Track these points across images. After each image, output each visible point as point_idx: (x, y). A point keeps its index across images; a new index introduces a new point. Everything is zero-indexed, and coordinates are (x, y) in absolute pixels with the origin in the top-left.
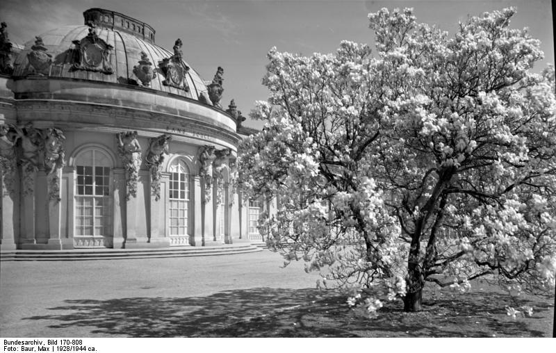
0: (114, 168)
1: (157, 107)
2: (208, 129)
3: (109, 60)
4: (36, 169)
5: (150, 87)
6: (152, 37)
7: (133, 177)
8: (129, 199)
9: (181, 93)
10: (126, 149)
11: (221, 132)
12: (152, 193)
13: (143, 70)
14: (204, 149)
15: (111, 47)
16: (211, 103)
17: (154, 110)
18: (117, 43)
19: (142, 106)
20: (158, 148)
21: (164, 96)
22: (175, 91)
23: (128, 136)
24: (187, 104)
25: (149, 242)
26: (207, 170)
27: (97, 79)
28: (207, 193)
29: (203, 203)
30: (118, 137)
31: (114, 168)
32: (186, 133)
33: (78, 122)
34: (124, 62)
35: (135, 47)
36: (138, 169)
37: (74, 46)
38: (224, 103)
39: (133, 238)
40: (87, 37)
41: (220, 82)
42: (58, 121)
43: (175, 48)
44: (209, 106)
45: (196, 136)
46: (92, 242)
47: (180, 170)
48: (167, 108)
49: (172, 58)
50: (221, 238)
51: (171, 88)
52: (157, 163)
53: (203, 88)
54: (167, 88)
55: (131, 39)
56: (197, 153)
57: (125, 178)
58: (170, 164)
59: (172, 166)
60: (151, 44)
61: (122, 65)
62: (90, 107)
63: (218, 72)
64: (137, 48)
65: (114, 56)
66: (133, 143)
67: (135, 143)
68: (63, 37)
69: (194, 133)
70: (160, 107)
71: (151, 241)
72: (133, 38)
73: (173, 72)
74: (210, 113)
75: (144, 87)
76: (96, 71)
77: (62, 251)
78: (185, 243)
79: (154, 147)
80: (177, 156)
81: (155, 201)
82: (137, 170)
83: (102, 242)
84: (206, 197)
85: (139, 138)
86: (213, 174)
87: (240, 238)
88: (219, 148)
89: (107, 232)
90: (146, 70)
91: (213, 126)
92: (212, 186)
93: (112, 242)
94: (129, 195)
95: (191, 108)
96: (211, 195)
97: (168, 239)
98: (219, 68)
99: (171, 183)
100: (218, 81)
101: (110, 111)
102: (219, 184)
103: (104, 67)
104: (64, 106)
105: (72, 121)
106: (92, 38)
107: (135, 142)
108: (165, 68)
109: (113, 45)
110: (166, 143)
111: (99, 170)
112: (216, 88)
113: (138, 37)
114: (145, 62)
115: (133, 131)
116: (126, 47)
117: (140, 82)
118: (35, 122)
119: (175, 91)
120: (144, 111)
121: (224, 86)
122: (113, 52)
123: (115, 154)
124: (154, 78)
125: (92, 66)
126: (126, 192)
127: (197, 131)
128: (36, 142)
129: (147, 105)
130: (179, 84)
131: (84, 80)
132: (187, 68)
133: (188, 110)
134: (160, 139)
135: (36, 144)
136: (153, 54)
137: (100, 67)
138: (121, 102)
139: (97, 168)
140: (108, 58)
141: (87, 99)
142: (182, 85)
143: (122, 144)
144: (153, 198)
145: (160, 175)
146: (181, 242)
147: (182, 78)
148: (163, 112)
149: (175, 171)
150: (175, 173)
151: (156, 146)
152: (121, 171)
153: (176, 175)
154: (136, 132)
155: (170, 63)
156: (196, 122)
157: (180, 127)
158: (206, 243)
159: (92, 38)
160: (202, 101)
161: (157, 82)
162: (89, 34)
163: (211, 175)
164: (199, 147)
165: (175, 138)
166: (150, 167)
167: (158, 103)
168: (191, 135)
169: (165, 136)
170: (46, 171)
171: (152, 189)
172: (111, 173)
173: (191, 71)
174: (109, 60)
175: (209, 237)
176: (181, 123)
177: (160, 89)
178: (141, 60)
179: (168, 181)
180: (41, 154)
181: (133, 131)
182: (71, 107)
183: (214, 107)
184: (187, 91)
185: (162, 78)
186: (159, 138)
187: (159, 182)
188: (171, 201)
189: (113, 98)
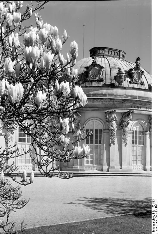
0: (104, 130)
1: (126, 96)
3: (102, 74)
6: (124, 56)
7: (113, 134)
9: (140, 86)
10: (110, 120)
12: (123, 142)
13: (118, 78)
15: (103, 67)
17: (124, 97)
18: (106, 64)
19: (118, 96)
20: (127, 118)
22: (136, 86)
23: (111, 113)
27: (96, 85)
30: (106, 114)
31: (104, 130)
32: (141, 109)
33: (87, 108)
34: (110, 74)
35: (115, 65)
36: (116, 129)
37: (86, 69)
39: (113, 166)
40: (92, 64)
43: (136, 62)
46: (93, 168)
47: (137, 129)
48: (131, 96)
49: (134, 68)
51: (134, 84)
52: (126, 126)
54: (132, 84)
57: (109, 135)
59: (134, 127)
61: (107, 75)
62: (92, 100)
64: (116, 65)
65: (104, 72)
66: (113, 116)
67: (115, 116)
68: (81, 65)
70: (127, 96)
71: (122, 168)
73: (135, 76)
75: (119, 86)
76: (95, 81)
77: (79, 172)
78: (140, 169)
80: (136, 122)
81: (124, 147)
82: (115, 130)
83: (95, 168)
85: (117, 113)
89: (100, 163)
90: (120, 77)
93: (103, 168)
94: (111, 144)
97: (131, 167)
99: (133, 136)
101: (102, 101)
103: (100, 78)
106: (94, 64)
107: (114, 115)
109: (104, 66)
110: (130, 115)
114: (120, 72)
115: (113, 110)
116: (111, 66)
117: (117, 84)
119: (136, 86)
120: (119, 99)
122: (104, 69)
123: (104, 123)
124: (125, 80)
125: (94, 78)
126: (110, 141)
130: (138, 82)
131: (90, 87)
132: (143, 72)
133: (143, 96)
134: (127, 113)
137: (97, 78)
138: (107, 95)
139: (95, 130)
141: (91, 96)
142: (140, 82)
143: (108, 117)
144: (123, 145)
145: (127, 132)
147: (140, 78)
148: (129, 98)
149: (135, 130)
150: (135, 131)
151: (125, 117)
152: (107, 131)
153: (136, 132)
154: (115, 111)
155: (133, 71)
157: (139, 105)
159: (94, 64)
162: (93, 63)
165: (135, 112)
166: (122, 128)
167: (127, 94)
169: (130, 111)
171: (123, 140)
172: (103, 132)
174: (102, 74)
176: (139, 104)
178: (118, 72)
179: (131, 135)
181: (113, 110)
184: (142, 85)
185: (129, 80)
186: (127, 112)
187: (126, 136)
188: (133, 146)
189: (104, 94)
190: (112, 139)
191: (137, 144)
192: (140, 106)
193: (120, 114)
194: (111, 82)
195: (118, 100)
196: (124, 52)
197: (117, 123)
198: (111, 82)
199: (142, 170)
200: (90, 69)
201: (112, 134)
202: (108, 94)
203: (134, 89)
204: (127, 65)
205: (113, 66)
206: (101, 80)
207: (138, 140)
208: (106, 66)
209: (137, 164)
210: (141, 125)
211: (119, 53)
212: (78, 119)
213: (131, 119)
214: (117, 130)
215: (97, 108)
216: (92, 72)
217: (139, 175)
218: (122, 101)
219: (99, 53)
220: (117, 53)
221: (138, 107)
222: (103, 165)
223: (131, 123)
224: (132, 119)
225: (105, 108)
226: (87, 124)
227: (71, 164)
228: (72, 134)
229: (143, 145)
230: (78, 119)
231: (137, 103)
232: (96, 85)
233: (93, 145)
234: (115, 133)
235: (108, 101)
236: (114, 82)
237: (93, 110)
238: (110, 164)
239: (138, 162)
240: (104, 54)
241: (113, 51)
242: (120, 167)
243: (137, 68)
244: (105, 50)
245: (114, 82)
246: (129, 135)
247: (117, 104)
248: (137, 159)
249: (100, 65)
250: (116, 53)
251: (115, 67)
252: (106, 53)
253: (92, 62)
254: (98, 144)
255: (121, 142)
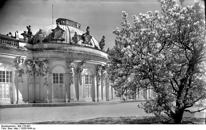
0: (66, 74)
2: (99, 59)
4: (40, 75)
5: (78, 44)
8: (71, 85)
9: (90, 46)
10: (70, 67)
11: (103, 59)
13: (75, 38)
14: (97, 66)
16: (100, 49)
18: (67, 30)
19: (75, 51)
20: (81, 66)
21: (83, 47)
22: (87, 45)
24: (92, 50)
25: (78, 100)
26: (99, 73)
28: (99, 82)
29: (98, 86)
32: (91, 61)
33: (53, 58)
34: (69, 36)
35: (73, 30)
36: (74, 73)
37: (52, 31)
38: (105, 49)
39: (72, 99)
40: (56, 28)
41: (104, 42)
42: (47, 58)
43: (87, 30)
44: (99, 50)
45: (95, 61)
48: (84, 51)
50: (105, 98)
52: (81, 71)
53: (97, 44)
54: (84, 44)
55: (71, 28)
56: (95, 67)
57: (69, 77)
58: (85, 71)
60: (79, 29)
62: (57, 52)
63: (103, 38)
64: (73, 30)
65: (65, 34)
66: (72, 64)
67: (73, 65)
68: (49, 29)
69: (94, 60)
70: (81, 51)
72: (72, 28)
73: (86, 38)
74: (100, 53)
77: (48, 103)
79: (79, 65)
80: (87, 69)
84: (99, 83)
86: (101, 75)
87: (112, 99)
88: (103, 65)
90: (76, 38)
91: (101, 57)
92: (101, 79)
94: (71, 83)
95: (93, 51)
96: (101, 83)
98: (103, 36)
99: (86, 79)
100: (103, 40)
101: (64, 53)
102: (104, 79)
104: (48, 52)
105: (51, 58)
106: (58, 28)
108: (83, 37)
109: (65, 30)
111: (61, 75)
112: (102, 43)
113: (74, 27)
116: (70, 31)
117: (74, 42)
118: (39, 59)
119: (87, 45)
121: (105, 43)
123: (66, 69)
124: (79, 41)
127: (95, 59)
128: (40, 65)
129: (77, 51)
132: (91, 37)
135: (40, 66)
136: (79, 33)
140: (63, 35)
141: (56, 50)
142: (89, 43)
144: (79, 84)
145: (82, 76)
146: (90, 100)
147: (90, 40)
148: (83, 53)
151: (80, 65)
152: (68, 75)
153: (88, 76)
156: (95, 56)
157: (89, 58)
158: (99, 100)
159: (58, 28)
160: (96, 48)
161: (80, 42)
163: (101, 75)
164: (96, 65)
166: (78, 73)
168: (93, 61)
169: (83, 61)
170: (43, 76)
173: (93, 38)
175: (100, 98)
177: (81, 45)
179: (85, 78)
180: (41, 70)
182: (51, 53)
183: (102, 50)
184: (91, 45)
185: (82, 41)
186: (81, 62)
188: (86, 85)
190: (71, 80)
191: (88, 84)
192: (90, 58)
193: (77, 63)
194: (70, 42)
195: (75, 54)
196: (79, 24)
197: (74, 69)
198: (70, 42)
199: (92, 101)
200: (55, 31)
201: (71, 76)
202: (68, 49)
203: (86, 47)
204: (81, 32)
205: (72, 31)
206: (64, 40)
207: (89, 81)
208: (67, 31)
209: (89, 97)
210: (91, 71)
211: (76, 25)
212: (47, 65)
213: (84, 67)
214: (75, 74)
215: (60, 59)
216: (57, 34)
217: (91, 104)
218: (78, 54)
219: (62, 23)
220: (75, 24)
221: (88, 59)
222: (65, 98)
223: (84, 70)
224: (84, 67)
225: (66, 58)
226: (54, 69)
227: (42, 98)
228: (43, 76)
229: (93, 84)
230: (47, 65)
231: (88, 56)
232: (60, 42)
233: (58, 85)
234: (74, 76)
235: (68, 54)
236: (72, 41)
237: (58, 60)
238: (71, 97)
239: (90, 96)
240: (66, 23)
241: (72, 22)
242: (77, 99)
243: (88, 33)
244: (66, 21)
245: (72, 41)
246: (83, 77)
247: (75, 56)
248: (89, 94)
249: (63, 29)
250: (75, 24)
251: (73, 32)
252: (67, 23)
253: (57, 26)
254: (62, 84)
255: (78, 82)
